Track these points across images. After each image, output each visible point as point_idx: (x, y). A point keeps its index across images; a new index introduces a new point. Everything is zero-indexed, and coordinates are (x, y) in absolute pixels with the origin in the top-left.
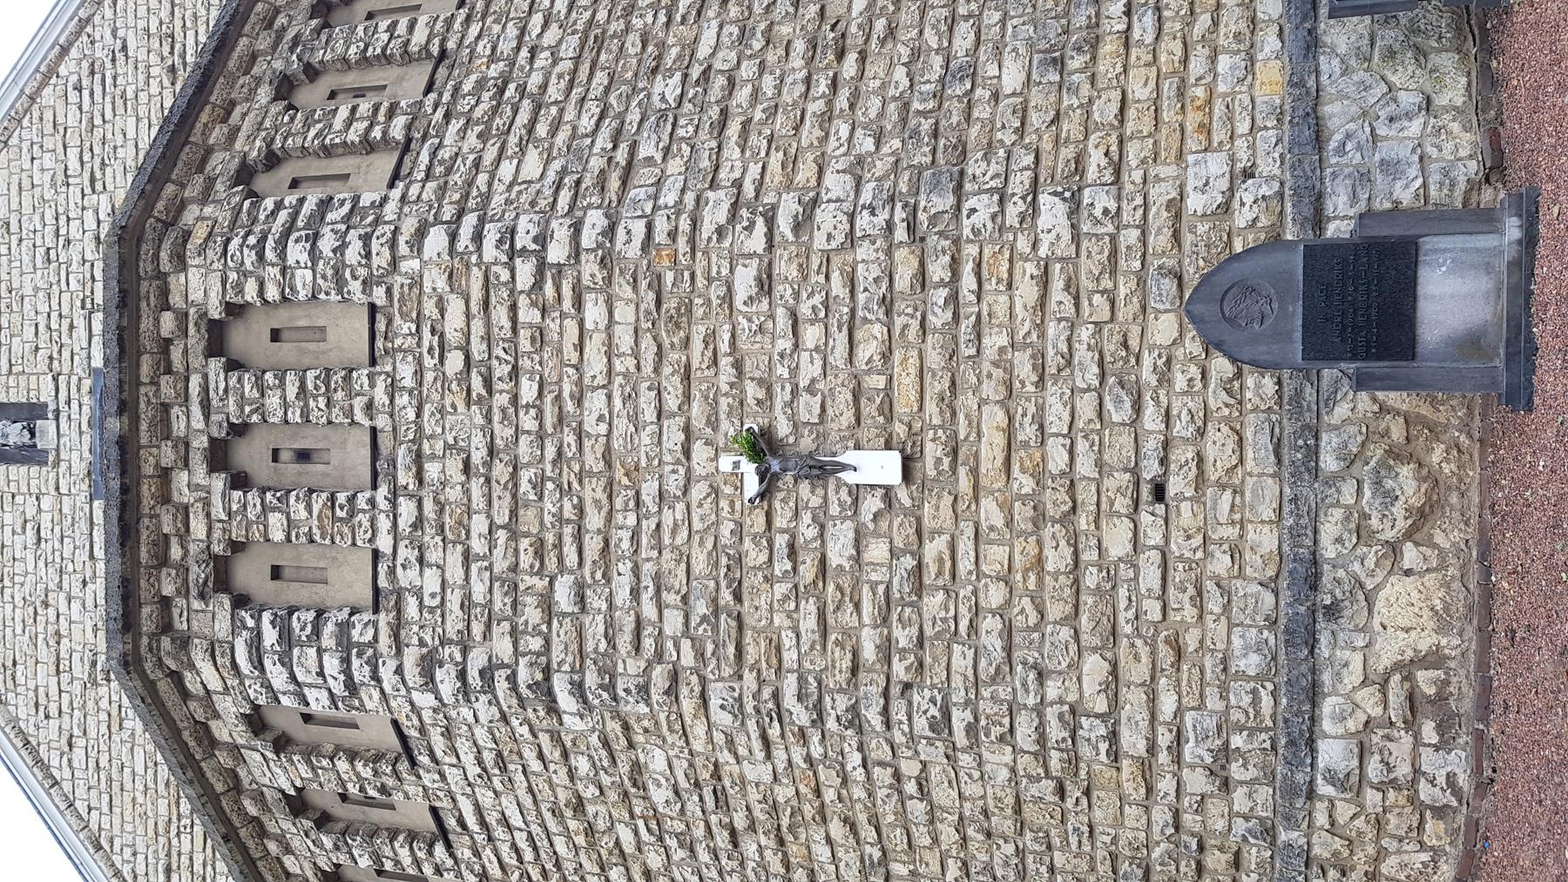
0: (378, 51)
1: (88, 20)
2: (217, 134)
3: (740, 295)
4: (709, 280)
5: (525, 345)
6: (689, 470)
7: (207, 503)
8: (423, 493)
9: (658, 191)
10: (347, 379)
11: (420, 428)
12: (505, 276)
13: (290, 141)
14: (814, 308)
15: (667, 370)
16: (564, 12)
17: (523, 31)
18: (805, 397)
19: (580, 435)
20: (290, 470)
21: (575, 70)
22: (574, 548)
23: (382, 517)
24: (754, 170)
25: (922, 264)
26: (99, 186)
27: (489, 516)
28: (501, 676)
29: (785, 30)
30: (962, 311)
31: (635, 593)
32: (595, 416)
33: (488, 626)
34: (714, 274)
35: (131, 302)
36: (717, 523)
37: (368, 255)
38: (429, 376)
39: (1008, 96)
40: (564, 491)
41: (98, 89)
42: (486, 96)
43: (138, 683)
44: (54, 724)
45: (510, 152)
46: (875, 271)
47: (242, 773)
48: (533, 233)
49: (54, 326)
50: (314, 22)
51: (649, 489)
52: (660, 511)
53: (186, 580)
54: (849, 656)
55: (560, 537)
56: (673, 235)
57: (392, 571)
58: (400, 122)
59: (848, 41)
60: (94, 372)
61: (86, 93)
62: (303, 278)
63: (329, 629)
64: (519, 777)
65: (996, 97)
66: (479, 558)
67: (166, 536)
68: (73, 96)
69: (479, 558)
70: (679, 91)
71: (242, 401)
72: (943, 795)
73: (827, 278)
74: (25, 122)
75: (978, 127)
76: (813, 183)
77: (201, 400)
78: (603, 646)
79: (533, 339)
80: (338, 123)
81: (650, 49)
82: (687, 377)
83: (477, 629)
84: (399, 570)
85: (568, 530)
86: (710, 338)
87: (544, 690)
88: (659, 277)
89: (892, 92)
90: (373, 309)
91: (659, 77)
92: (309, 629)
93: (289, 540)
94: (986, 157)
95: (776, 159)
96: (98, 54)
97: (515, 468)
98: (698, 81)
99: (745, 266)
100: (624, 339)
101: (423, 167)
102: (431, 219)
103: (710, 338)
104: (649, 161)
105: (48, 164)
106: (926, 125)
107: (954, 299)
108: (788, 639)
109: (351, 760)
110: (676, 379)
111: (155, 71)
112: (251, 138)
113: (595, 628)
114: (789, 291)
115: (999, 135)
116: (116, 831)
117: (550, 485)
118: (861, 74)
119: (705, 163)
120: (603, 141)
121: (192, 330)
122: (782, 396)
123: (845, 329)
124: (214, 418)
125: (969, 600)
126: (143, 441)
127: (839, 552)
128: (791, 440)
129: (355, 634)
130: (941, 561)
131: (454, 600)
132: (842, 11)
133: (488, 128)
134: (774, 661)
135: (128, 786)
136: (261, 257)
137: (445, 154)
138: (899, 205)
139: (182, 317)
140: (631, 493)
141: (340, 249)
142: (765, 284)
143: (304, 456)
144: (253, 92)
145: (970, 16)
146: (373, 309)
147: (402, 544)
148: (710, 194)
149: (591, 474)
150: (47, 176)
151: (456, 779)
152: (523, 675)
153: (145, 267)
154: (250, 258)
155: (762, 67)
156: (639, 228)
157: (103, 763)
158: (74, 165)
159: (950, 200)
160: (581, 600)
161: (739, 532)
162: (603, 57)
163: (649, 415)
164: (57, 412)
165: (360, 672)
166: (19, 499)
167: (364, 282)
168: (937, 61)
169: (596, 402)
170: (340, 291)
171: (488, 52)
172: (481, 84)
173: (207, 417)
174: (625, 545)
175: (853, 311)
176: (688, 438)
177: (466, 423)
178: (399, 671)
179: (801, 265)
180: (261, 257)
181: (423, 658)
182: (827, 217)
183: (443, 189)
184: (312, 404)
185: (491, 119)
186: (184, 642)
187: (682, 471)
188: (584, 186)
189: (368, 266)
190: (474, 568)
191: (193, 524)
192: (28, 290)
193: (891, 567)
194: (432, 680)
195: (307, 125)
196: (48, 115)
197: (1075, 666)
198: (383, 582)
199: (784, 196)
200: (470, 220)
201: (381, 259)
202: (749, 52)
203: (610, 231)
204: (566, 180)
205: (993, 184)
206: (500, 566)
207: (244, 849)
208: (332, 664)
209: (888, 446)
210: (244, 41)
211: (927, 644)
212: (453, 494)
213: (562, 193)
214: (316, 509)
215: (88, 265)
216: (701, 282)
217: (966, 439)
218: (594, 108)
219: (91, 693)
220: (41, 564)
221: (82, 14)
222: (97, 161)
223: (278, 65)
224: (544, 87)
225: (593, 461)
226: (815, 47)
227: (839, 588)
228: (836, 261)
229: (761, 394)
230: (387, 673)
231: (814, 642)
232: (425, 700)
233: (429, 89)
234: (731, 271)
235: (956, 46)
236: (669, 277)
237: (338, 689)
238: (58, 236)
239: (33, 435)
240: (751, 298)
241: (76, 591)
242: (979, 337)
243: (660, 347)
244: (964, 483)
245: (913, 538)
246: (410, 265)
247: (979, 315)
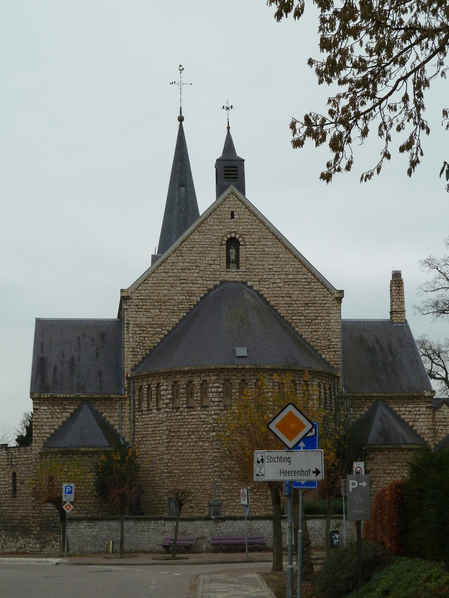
26: (285, 283)
44: (170, 267)
71: (251, 385)
72: (206, 481)
105: (291, 269)
111: (307, 299)
116: (149, 285)
129: (221, 403)
135: (159, 288)
151: (198, 412)
157: (163, 282)
164: (238, 272)
166: (219, 259)
197: (224, 496)
215: (269, 280)
220: (205, 265)
221: (320, 281)
238: (275, 272)
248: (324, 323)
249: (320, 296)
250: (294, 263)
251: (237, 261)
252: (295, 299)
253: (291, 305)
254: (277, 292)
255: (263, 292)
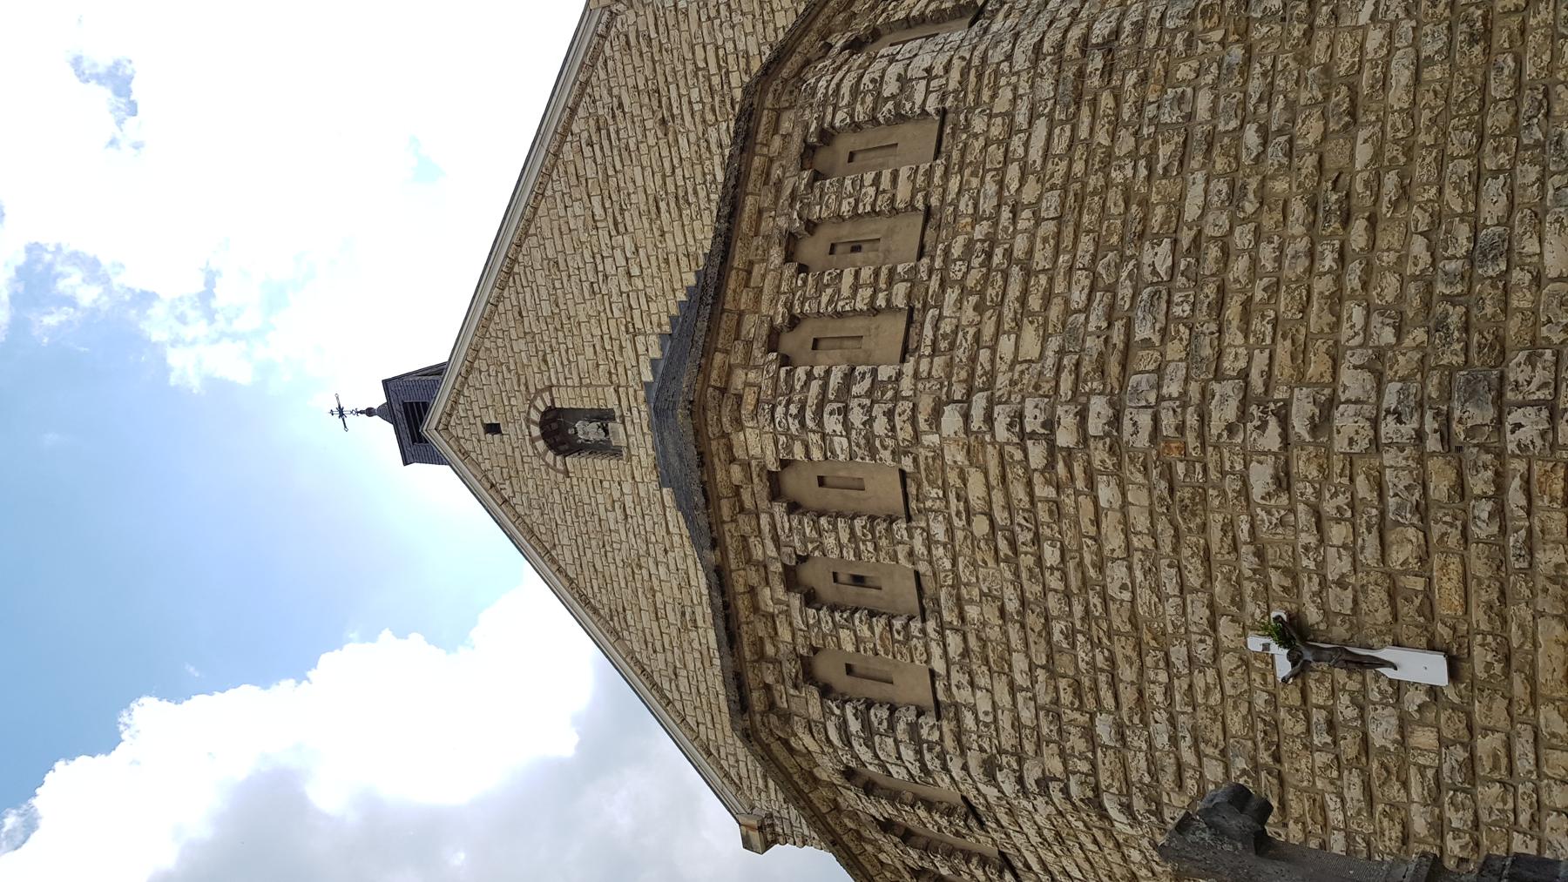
0: (868, 208)
1: (587, 82)
2: (745, 299)
3: (1257, 492)
4: (1223, 474)
5: (1043, 516)
6: (1216, 641)
7: (788, 614)
8: (967, 628)
9: (1161, 378)
10: (889, 530)
11: (957, 577)
12: (1018, 455)
13: (807, 307)
14: (1339, 508)
15: (1186, 552)
16: (1039, 162)
17: (1001, 184)
18: (1334, 591)
19: (1105, 599)
20: (851, 593)
21: (1059, 233)
22: (1109, 694)
23: (933, 644)
24: (1261, 359)
25: (1460, 475)
26: (622, 229)
27: (1028, 656)
28: (1055, 788)
29: (1280, 186)
30: (1509, 524)
31: (1174, 741)
32: (1117, 584)
33: (1038, 745)
34: (1227, 468)
35: (707, 459)
36: (1250, 691)
37: (893, 429)
38: (959, 535)
39: (1553, 280)
40: (1095, 644)
41: (606, 143)
42: (976, 262)
43: (758, 748)
45: (1006, 327)
46: (1405, 479)
47: (840, 800)
48: (1041, 419)
49: (608, 347)
50: (806, 174)
51: (1178, 653)
52: (1191, 673)
53: (781, 671)
54: (1399, 827)
55: (1095, 681)
56: (1181, 428)
57: (948, 688)
58: (900, 289)
59: (1354, 201)
60: (647, 386)
61: (597, 147)
62: (840, 443)
63: (901, 727)
64: (1076, 850)
65: (1538, 280)
66: (1022, 689)
67: (761, 639)
68: (587, 151)
69: (1022, 689)
70: (1169, 262)
71: (805, 540)
73: (1352, 480)
74: (555, 177)
75: (1518, 318)
76: (1327, 378)
77: (770, 535)
78: (1147, 779)
79: (1051, 512)
80: (846, 291)
81: (1134, 208)
82: (1207, 558)
83: (1029, 747)
84: (954, 689)
85: (1102, 678)
86: (1229, 527)
87: (1096, 803)
88: (1170, 466)
89: (1410, 270)
90: (903, 473)
91: (1147, 245)
92: (885, 724)
93: (858, 650)
94: (1531, 361)
95: (1283, 349)
96: (600, 112)
97: (1046, 619)
98: (1188, 250)
99: (1260, 463)
100: (1141, 522)
101: (928, 342)
102: (944, 397)
103: (1229, 527)
104: (1147, 343)
105: (578, 212)
106: (1455, 315)
107: (1500, 512)
108: (1332, 803)
109: (929, 811)
110: (1196, 561)
111: (649, 124)
112: (774, 302)
113: (1139, 763)
114: (1310, 490)
115: (1544, 331)
116: (721, 742)
117: (1080, 638)
118: (1373, 241)
119: (1207, 352)
120: (1096, 320)
121: (756, 480)
122: (1309, 586)
123: (1375, 530)
124: (784, 549)
125: (1529, 796)
126: (733, 567)
127: (1383, 731)
128: (1323, 627)
130: (1496, 757)
131: (1005, 720)
132: (1344, 161)
133: (983, 298)
134: (1319, 818)
136: (803, 424)
137: (946, 327)
138: (1429, 415)
139: (746, 466)
140: (1160, 655)
141: (869, 422)
142: (1283, 481)
143: (858, 580)
144: (766, 251)
145: (1500, 170)
146: (903, 473)
147: (954, 669)
148: (1215, 386)
149: (1119, 633)
150: (580, 224)
152: (1074, 789)
153: (713, 430)
154: (794, 427)
155: (1257, 232)
156: (1145, 420)
158: (598, 211)
159: (1490, 413)
160: (1122, 737)
161: (1273, 700)
162: (1085, 218)
163: (1171, 588)
164: (622, 417)
165: (932, 763)
166: (606, 484)
167: (893, 452)
168: (1463, 231)
169: (1118, 572)
170: (873, 458)
171: (971, 211)
172: (969, 246)
173: (778, 548)
174: (1159, 698)
175: (1383, 514)
176: (1213, 613)
177: (996, 576)
178: (965, 767)
179: (1321, 466)
180: (803, 424)
181: (984, 761)
182: (1346, 421)
183: (950, 365)
184: (862, 547)
185: (984, 288)
186: (786, 717)
187: (1209, 641)
188: (1084, 370)
189: (894, 437)
190: (1020, 697)
191: (780, 631)
192: (583, 318)
193: (1439, 754)
194: (995, 779)
195: (820, 288)
196: (571, 169)
198: (941, 697)
199: (1296, 390)
200: (979, 401)
201: (905, 433)
202: (1242, 215)
203: (1116, 421)
204: (1065, 362)
205: (1540, 395)
206: (1044, 699)
207: (847, 849)
208: (908, 754)
209: (1431, 647)
210: (750, 200)
211: (1482, 827)
212: (994, 633)
213: (1063, 376)
214: (877, 631)
216: (1214, 475)
217: (1521, 647)
218: (1083, 279)
219: (685, 636)
220: (631, 535)
221: (582, 78)
222: (617, 207)
223: (782, 222)
224: (1030, 252)
225: (1120, 622)
226: (1315, 209)
227: (1383, 765)
228: (1361, 466)
229: (1287, 583)
230: (955, 767)
231: (1360, 810)
232: (991, 793)
233: (921, 255)
234: (1246, 466)
235: (1484, 214)
236: (1180, 468)
237: (916, 771)
239: (606, 432)
240: (1268, 494)
241: (661, 558)
242: (1531, 553)
243: (1176, 529)
244: (1519, 688)
245: (1464, 732)
246: (931, 439)
247: (1530, 531)
248: (712, 31)
249: (629, 69)
250: (558, 195)
251: (603, 417)
252: (659, 181)
253: (681, 194)
254: (653, 259)
255: (665, 319)
